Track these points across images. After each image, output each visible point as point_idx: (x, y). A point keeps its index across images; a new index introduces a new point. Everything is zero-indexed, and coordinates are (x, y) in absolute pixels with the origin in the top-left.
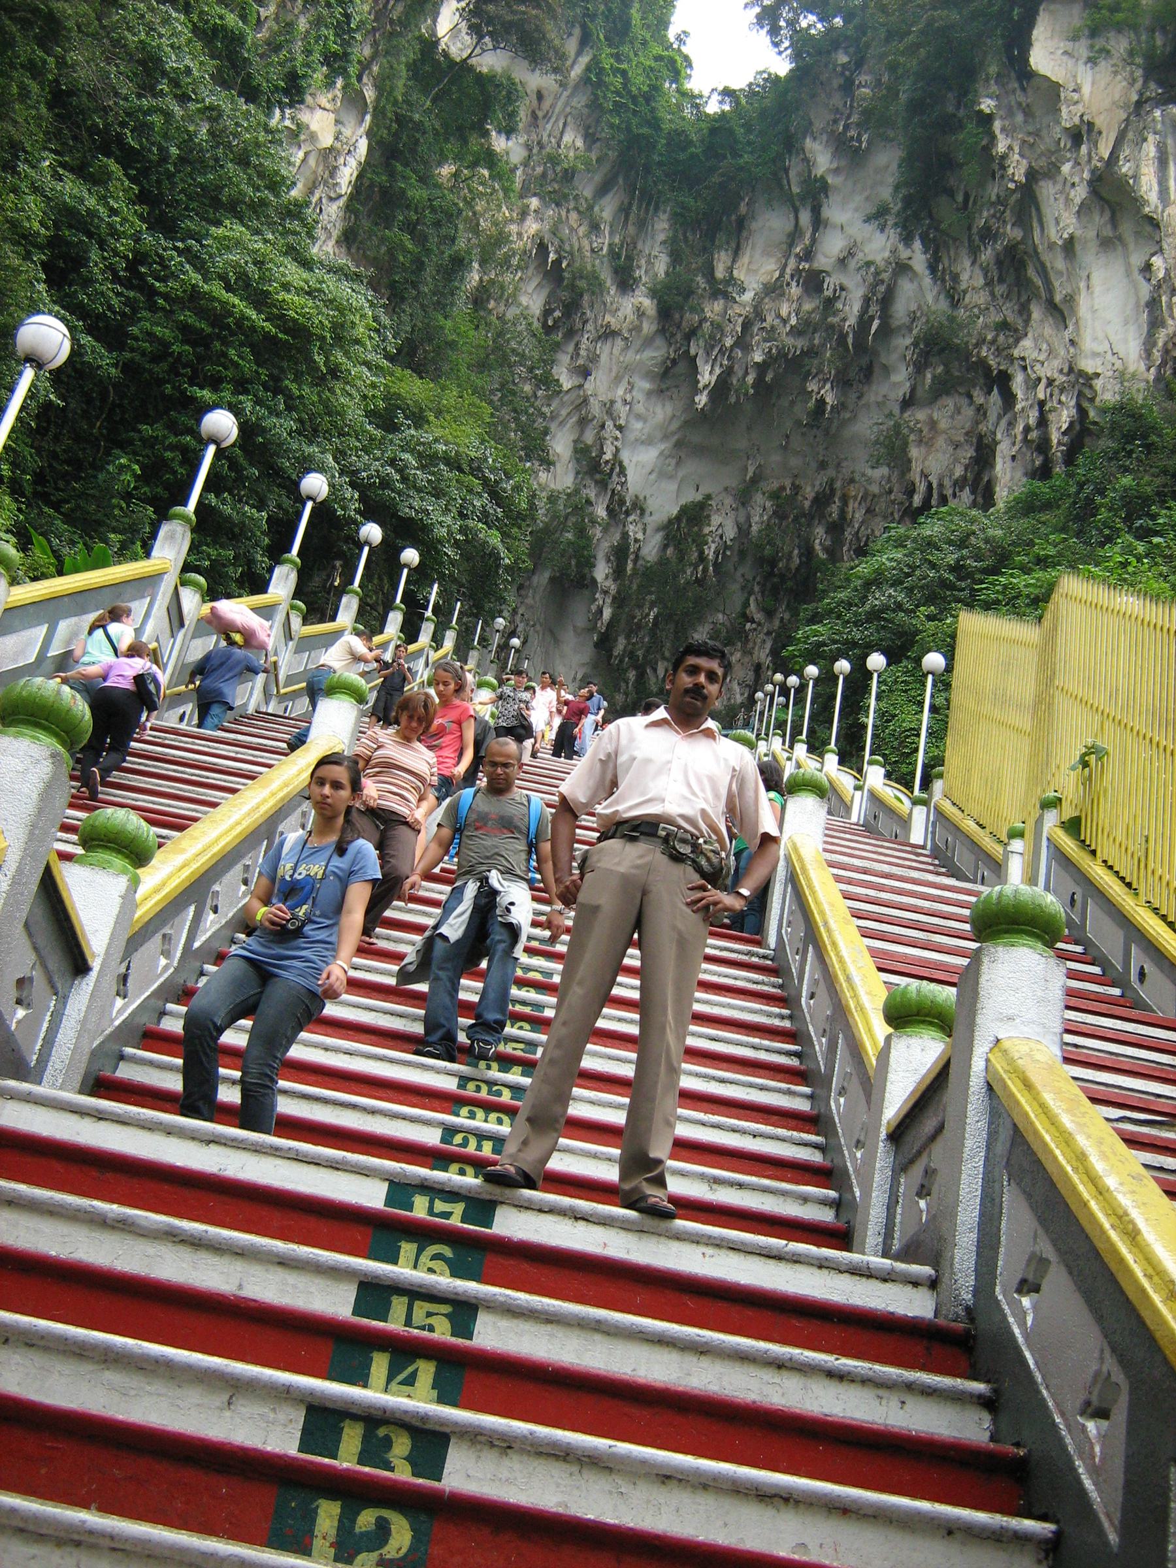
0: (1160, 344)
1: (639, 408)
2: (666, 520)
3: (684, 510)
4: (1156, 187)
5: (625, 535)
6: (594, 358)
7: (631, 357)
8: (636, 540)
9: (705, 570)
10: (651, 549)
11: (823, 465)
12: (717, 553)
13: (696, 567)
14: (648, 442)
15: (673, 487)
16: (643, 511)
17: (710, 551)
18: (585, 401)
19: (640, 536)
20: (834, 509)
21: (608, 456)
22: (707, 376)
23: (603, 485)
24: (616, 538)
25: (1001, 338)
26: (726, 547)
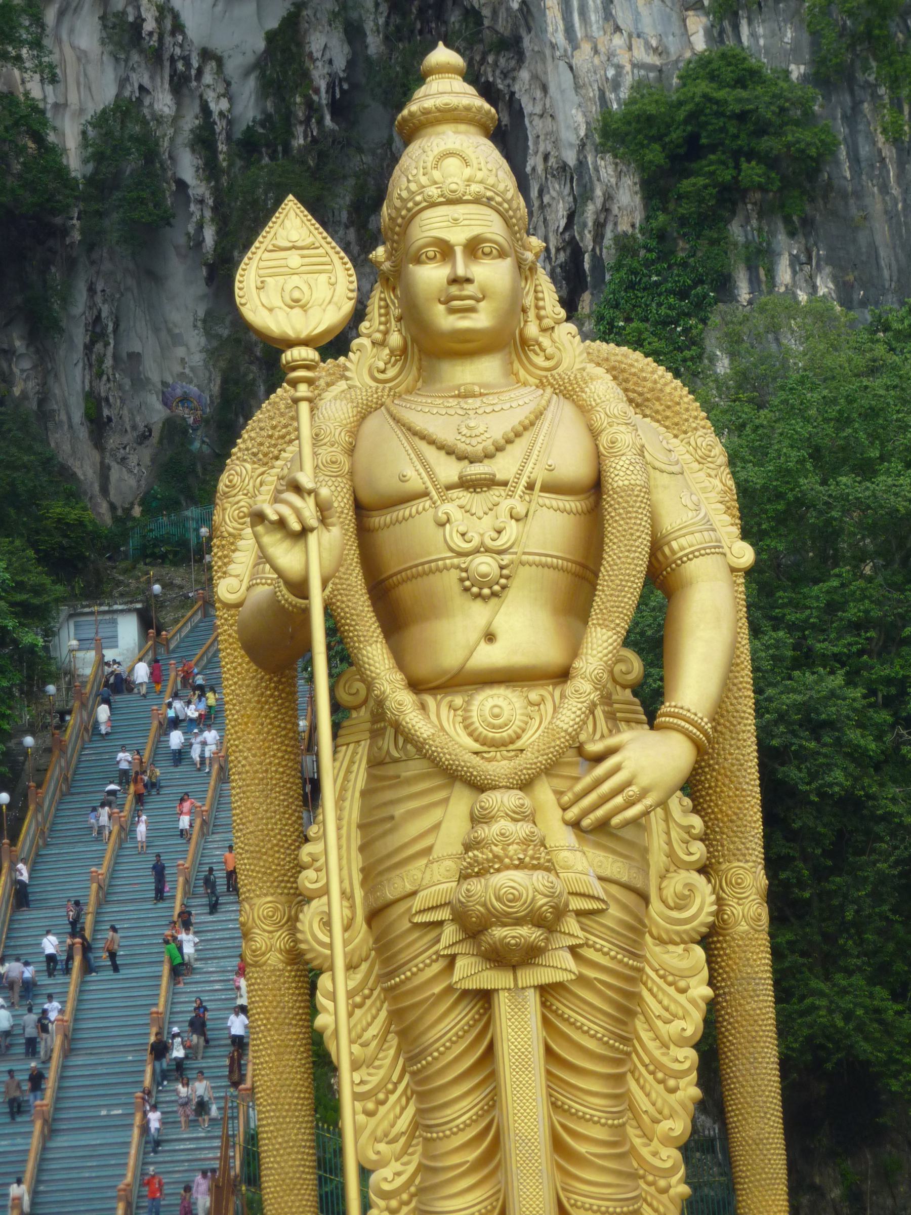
0: (590, 224)
2: (250, 59)
3: (271, 37)
4: (561, 26)
5: (205, 110)
8: (221, 114)
9: (320, 122)
12: (331, 88)
13: (307, 122)
16: (220, 61)
19: (224, 104)
21: (150, 25)
23: (156, 57)
24: (190, 121)
25: (502, 61)
26: (341, 80)
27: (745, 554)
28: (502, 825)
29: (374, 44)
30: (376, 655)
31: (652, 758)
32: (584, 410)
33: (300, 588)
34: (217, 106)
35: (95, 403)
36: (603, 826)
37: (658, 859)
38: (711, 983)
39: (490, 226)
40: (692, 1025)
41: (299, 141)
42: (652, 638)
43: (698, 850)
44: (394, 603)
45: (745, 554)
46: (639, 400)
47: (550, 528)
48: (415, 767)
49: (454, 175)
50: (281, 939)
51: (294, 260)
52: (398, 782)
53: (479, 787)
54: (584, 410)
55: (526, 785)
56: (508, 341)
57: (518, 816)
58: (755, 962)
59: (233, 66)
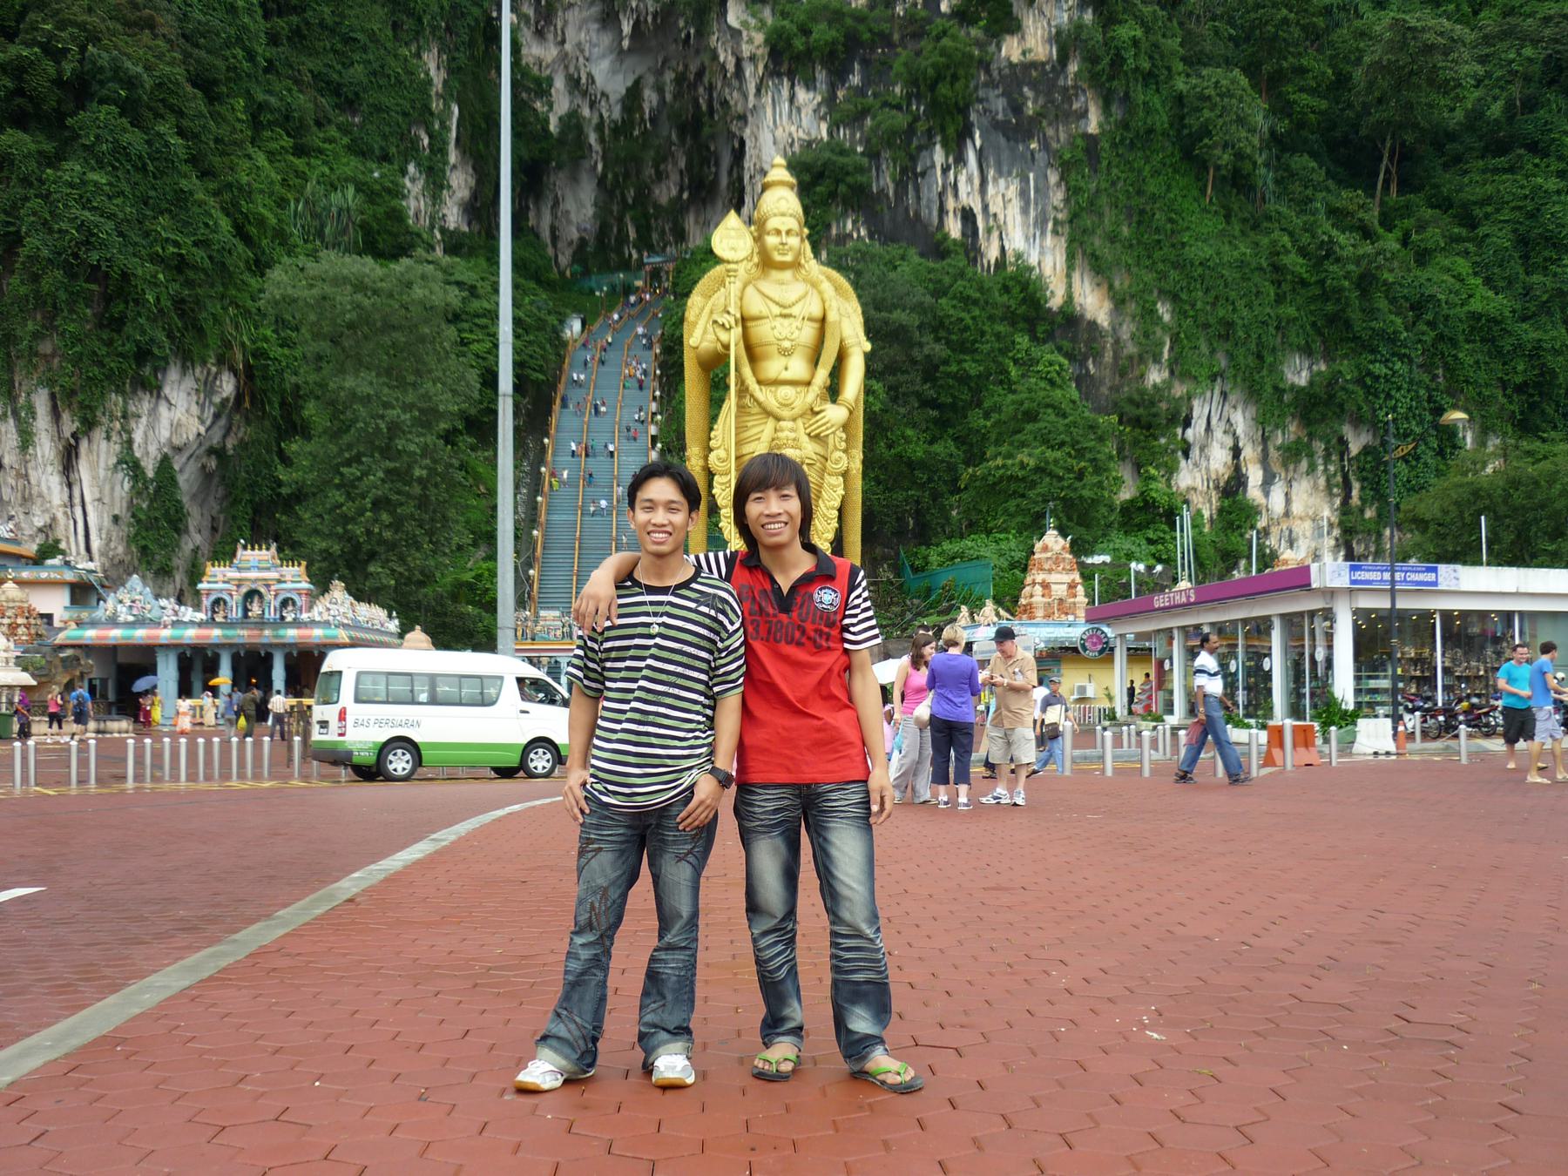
1: (595, 39)
3: (628, 90)
5: (601, 116)
6: (566, 22)
7: (586, 14)
10: (617, 113)
11: (697, 52)
14: (604, 56)
15: (620, 77)
17: (647, 116)
18: (566, 54)
20: (706, 80)
21: (584, 80)
22: (627, 28)
23: (585, 94)
24: (595, 120)
27: (868, 347)
28: (786, 433)
29: (668, 97)
30: (747, 371)
31: (835, 414)
32: (820, 293)
33: (727, 347)
34: (606, 115)
35: (553, 229)
36: (817, 436)
37: (831, 447)
38: (845, 488)
39: (793, 224)
40: (837, 504)
41: (636, 133)
42: (837, 373)
43: (844, 445)
44: (753, 353)
45: (868, 347)
46: (837, 289)
47: (808, 333)
48: (756, 410)
49: (783, 206)
50: (701, 462)
51: (733, 233)
52: (750, 414)
53: (778, 419)
54: (820, 293)
55: (794, 420)
56: (795, 265)
57: (792, 430)
58: (858, 484)
59: (613, 98)
